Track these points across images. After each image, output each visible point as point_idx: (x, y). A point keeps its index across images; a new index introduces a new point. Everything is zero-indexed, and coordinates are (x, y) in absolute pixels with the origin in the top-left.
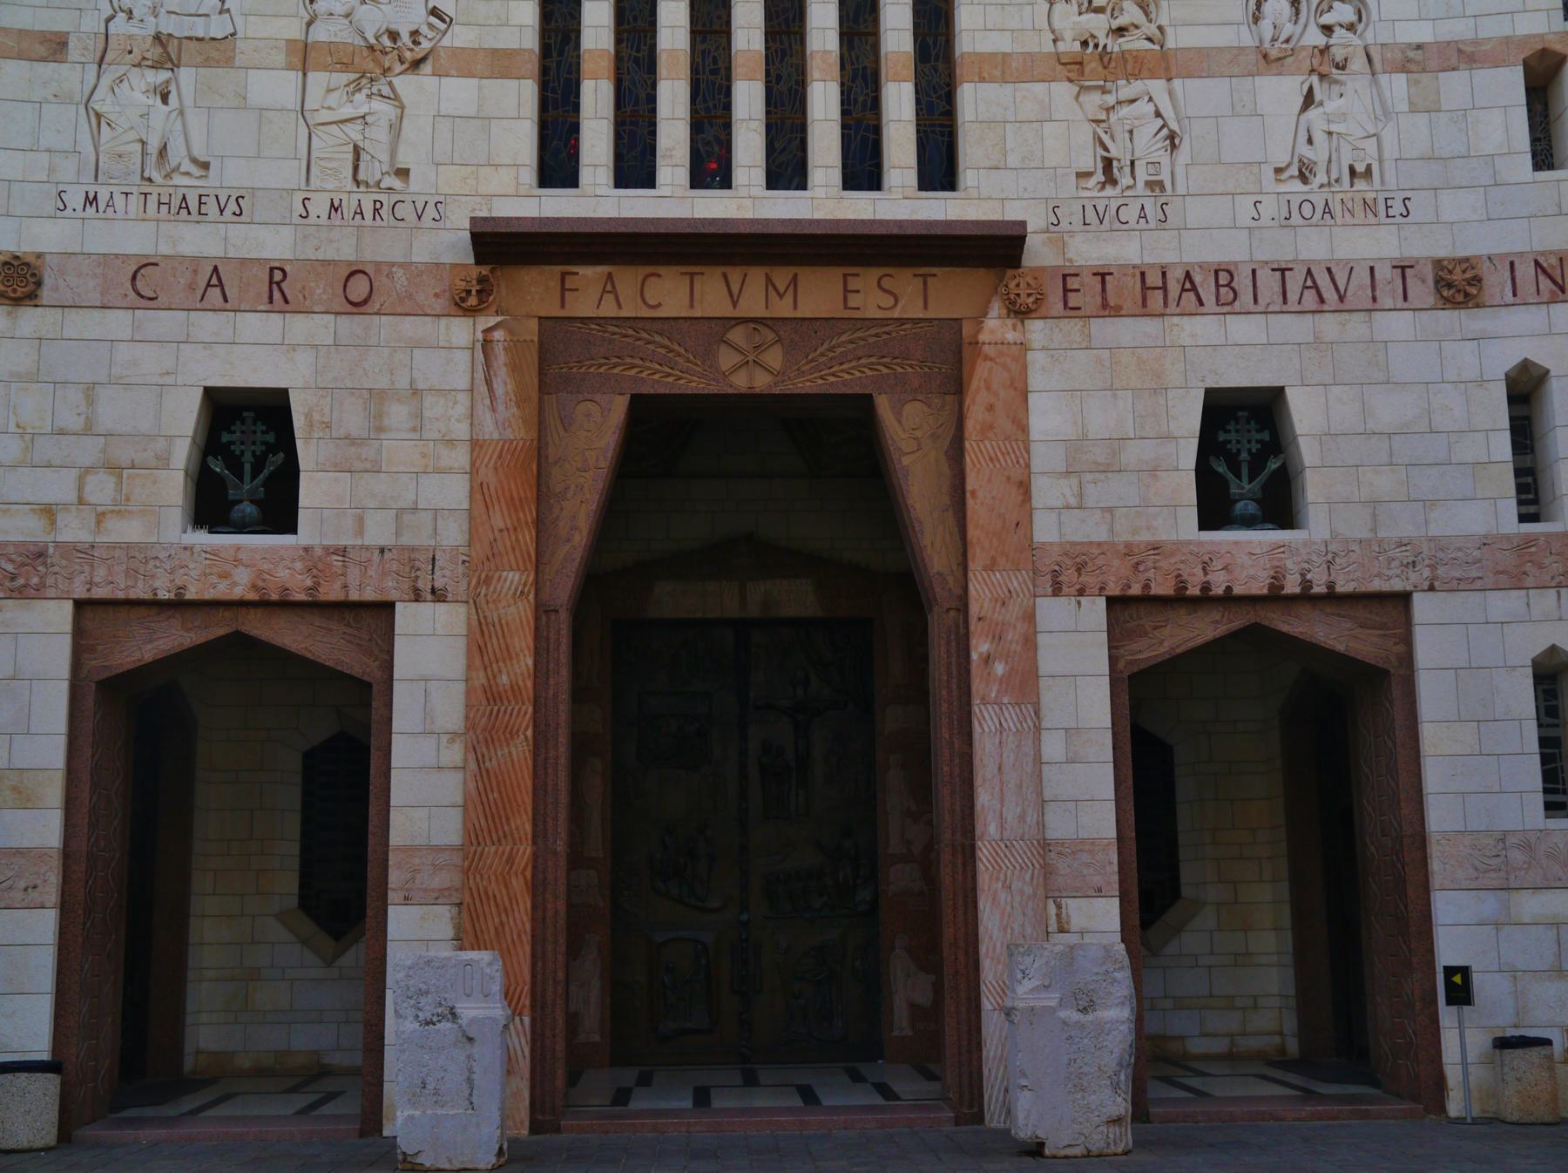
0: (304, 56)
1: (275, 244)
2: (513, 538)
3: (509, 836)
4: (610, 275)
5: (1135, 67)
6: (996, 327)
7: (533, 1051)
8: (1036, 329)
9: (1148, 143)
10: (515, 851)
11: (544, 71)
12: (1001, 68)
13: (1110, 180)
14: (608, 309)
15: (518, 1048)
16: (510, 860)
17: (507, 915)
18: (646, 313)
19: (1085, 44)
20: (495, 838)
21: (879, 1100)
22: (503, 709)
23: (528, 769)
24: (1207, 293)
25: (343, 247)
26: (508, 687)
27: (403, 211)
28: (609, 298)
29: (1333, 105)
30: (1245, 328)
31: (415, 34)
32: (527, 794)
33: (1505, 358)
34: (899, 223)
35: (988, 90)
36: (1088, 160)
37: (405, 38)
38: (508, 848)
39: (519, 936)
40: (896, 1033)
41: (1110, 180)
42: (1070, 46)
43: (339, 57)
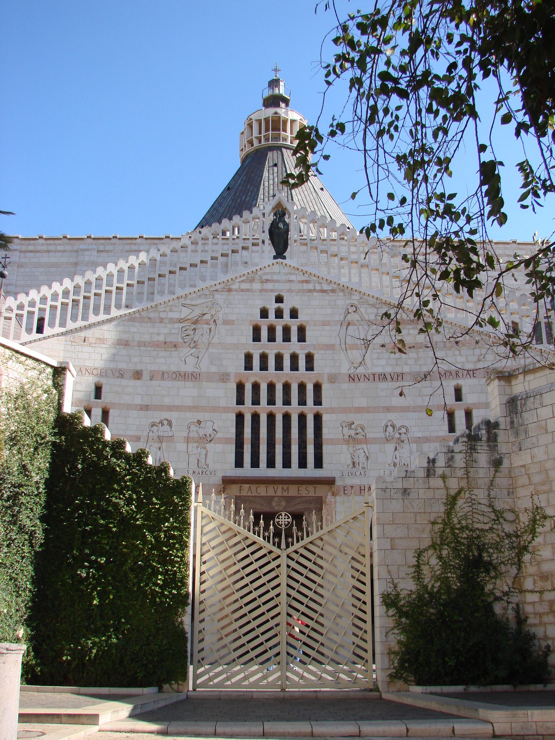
0: (188, 440)
4: (250, 487)
5: (359, 442)
6: (329, 498)
8: (338, 498)
9: (362, 459)
11: (236, 440)
12: (332, 442)
13: (354, 466)
14: (249, 494)
18: (257, 495)
19: (349, 436)
27: (208, 473)
28: (250, 491)
31: (210, 435)
34: (309, 477)
35: (329, 447)
36: (349, 462)
37: (208, 436)
41: (354, 466)
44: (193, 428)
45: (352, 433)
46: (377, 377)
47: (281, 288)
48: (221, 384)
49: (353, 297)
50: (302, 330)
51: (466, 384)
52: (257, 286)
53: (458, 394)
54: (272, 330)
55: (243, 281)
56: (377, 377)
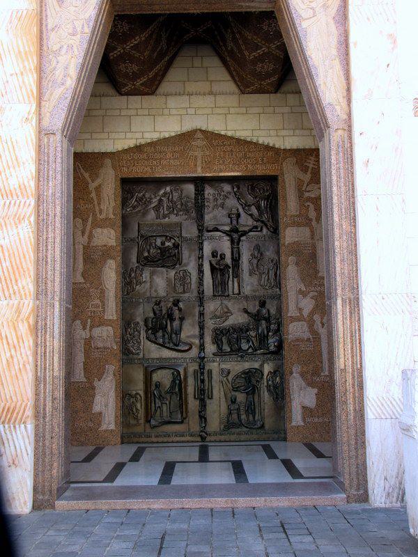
2: (21, 80)
3: (17, 293)
7: (36, 448)
10: (21, 305)
15: (23, 448)
16: (18, 311)
17: (15, 351)
20: (7, 293)
21: (288, 479)
22: (13, 202)
23: (31, 245)
26: (17, 186)
32: (31, 262)
38: (16, 302)
39: (24, 365)
40: (294, 424)
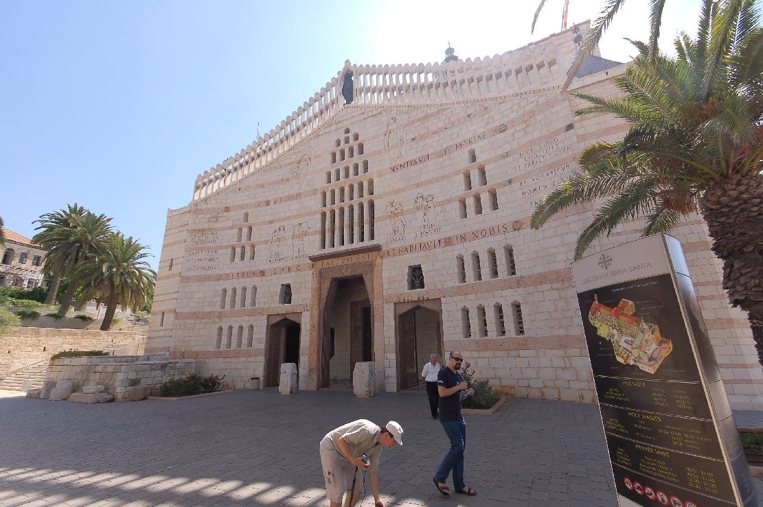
1: (289, 263)
6: (379, 261)
24: (409, 250)
25: (296, 262)
29: (428, 214)
30: (415, 255)
33: (456, 254)
42: (389, 213)
43: (298, 236)
44: (296, 229)
45: (393, 209)
46: (409, 163)
47: (346, 124)
48: (313, 197)
49: (393, 112)
50: (361, 147)
51: (475, 147)
52: (334, 127)
53: (473, 158)
54: (343, 153)
55: (326, 127)
56: (409, 163)
